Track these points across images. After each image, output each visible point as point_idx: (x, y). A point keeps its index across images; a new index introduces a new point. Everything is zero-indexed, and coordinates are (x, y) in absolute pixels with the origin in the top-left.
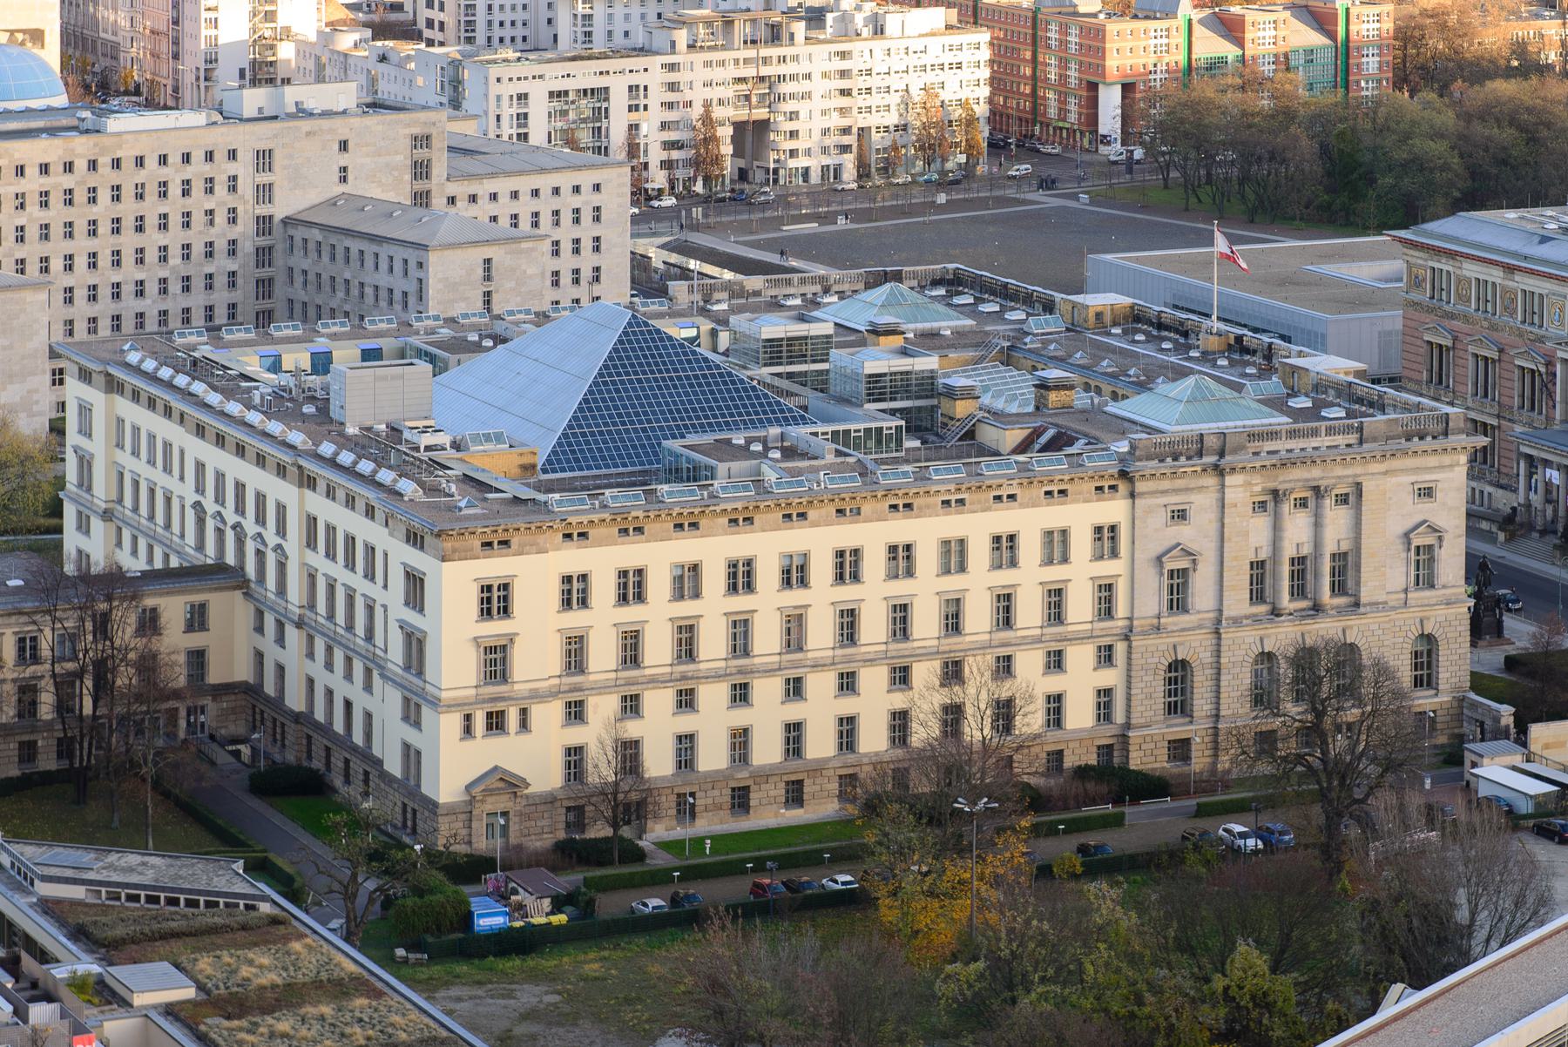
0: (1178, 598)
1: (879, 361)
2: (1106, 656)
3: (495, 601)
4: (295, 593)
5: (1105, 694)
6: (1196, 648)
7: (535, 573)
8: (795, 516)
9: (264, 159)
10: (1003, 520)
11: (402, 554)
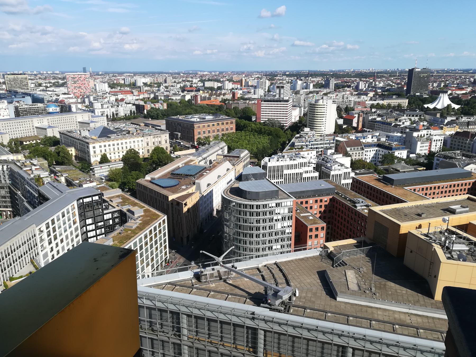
0: (148, 145)
3: (94, 147)
4: (79, 148)
6: (150, 148)
7: (97, 145)
8: (117, 140)
9: (76, 117)
11: (86, 144)
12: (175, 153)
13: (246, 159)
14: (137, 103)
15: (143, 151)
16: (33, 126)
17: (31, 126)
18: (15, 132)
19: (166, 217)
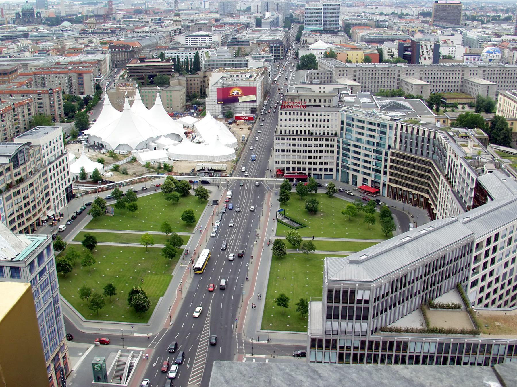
16: (462, 78)
17: (460, 78)
18: (439, 84)
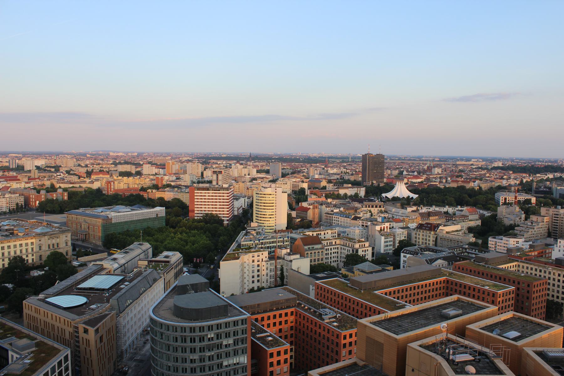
1: (6, 227)
2: (33, 255)
5: (33, 259)
6: (43, 253)
10: (20, 242)
12: (79, 259)
13: (179, 264)
14: (25, 192)
15: (34, 257)
19: (69, 352)
